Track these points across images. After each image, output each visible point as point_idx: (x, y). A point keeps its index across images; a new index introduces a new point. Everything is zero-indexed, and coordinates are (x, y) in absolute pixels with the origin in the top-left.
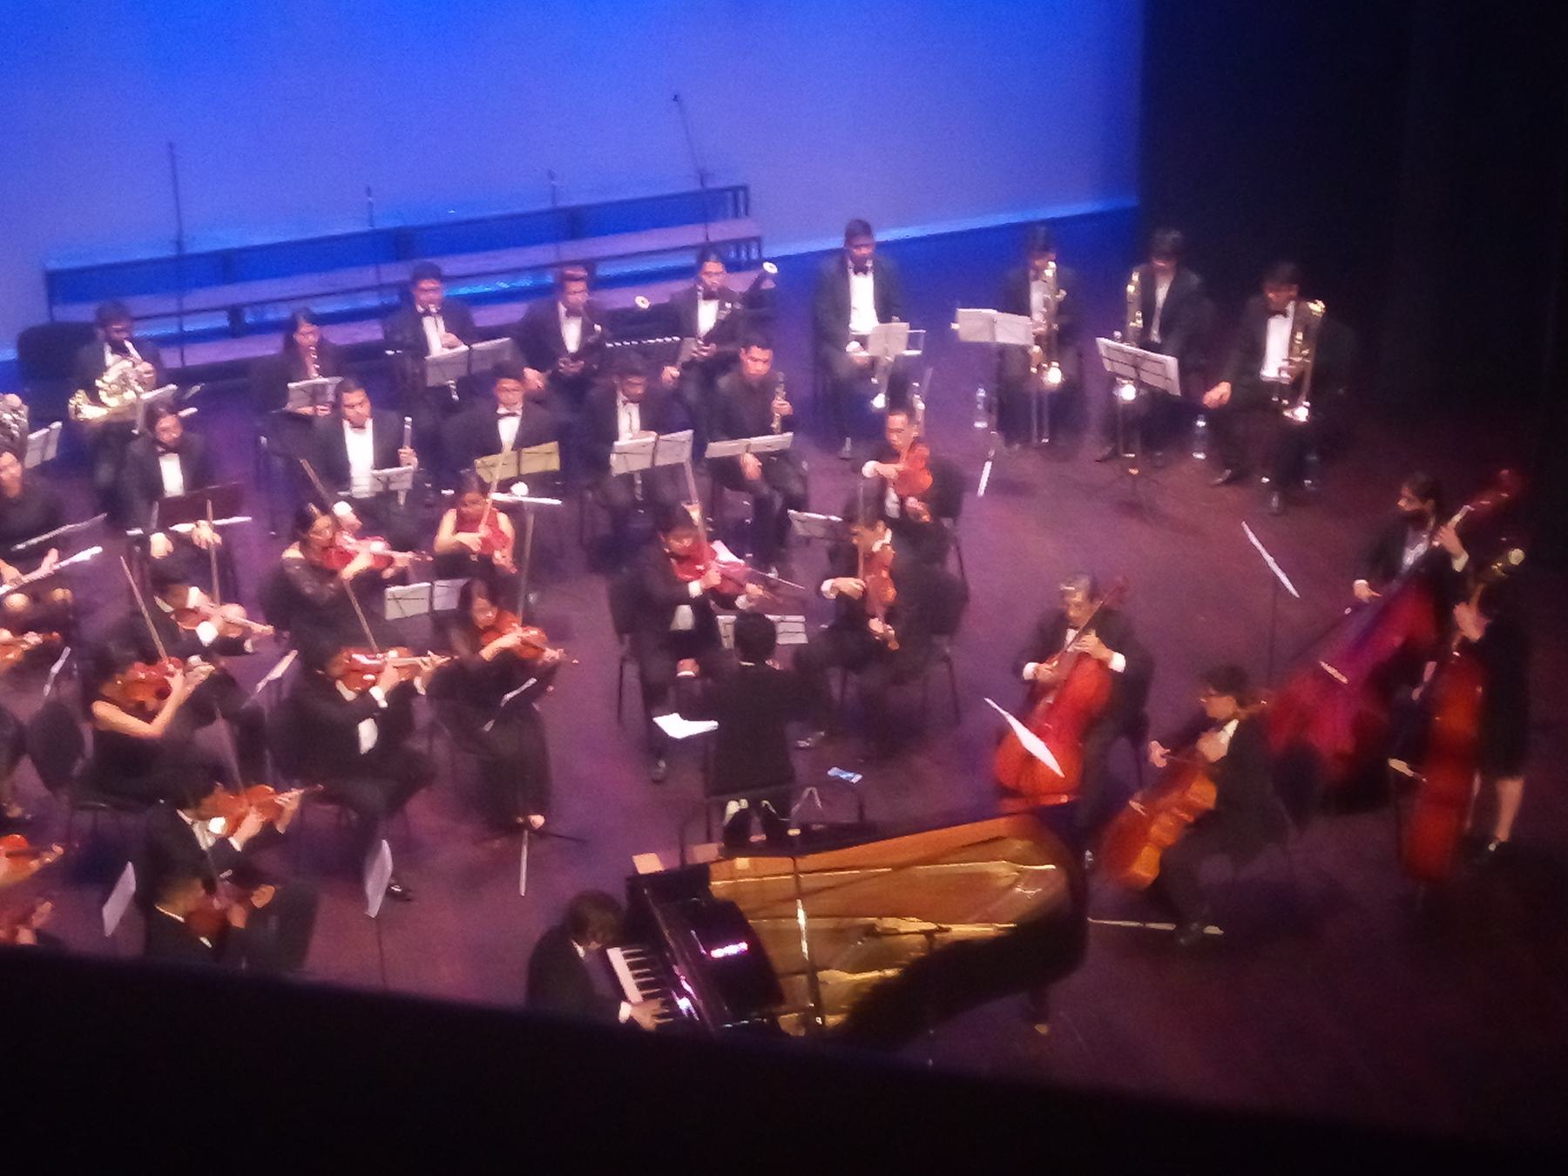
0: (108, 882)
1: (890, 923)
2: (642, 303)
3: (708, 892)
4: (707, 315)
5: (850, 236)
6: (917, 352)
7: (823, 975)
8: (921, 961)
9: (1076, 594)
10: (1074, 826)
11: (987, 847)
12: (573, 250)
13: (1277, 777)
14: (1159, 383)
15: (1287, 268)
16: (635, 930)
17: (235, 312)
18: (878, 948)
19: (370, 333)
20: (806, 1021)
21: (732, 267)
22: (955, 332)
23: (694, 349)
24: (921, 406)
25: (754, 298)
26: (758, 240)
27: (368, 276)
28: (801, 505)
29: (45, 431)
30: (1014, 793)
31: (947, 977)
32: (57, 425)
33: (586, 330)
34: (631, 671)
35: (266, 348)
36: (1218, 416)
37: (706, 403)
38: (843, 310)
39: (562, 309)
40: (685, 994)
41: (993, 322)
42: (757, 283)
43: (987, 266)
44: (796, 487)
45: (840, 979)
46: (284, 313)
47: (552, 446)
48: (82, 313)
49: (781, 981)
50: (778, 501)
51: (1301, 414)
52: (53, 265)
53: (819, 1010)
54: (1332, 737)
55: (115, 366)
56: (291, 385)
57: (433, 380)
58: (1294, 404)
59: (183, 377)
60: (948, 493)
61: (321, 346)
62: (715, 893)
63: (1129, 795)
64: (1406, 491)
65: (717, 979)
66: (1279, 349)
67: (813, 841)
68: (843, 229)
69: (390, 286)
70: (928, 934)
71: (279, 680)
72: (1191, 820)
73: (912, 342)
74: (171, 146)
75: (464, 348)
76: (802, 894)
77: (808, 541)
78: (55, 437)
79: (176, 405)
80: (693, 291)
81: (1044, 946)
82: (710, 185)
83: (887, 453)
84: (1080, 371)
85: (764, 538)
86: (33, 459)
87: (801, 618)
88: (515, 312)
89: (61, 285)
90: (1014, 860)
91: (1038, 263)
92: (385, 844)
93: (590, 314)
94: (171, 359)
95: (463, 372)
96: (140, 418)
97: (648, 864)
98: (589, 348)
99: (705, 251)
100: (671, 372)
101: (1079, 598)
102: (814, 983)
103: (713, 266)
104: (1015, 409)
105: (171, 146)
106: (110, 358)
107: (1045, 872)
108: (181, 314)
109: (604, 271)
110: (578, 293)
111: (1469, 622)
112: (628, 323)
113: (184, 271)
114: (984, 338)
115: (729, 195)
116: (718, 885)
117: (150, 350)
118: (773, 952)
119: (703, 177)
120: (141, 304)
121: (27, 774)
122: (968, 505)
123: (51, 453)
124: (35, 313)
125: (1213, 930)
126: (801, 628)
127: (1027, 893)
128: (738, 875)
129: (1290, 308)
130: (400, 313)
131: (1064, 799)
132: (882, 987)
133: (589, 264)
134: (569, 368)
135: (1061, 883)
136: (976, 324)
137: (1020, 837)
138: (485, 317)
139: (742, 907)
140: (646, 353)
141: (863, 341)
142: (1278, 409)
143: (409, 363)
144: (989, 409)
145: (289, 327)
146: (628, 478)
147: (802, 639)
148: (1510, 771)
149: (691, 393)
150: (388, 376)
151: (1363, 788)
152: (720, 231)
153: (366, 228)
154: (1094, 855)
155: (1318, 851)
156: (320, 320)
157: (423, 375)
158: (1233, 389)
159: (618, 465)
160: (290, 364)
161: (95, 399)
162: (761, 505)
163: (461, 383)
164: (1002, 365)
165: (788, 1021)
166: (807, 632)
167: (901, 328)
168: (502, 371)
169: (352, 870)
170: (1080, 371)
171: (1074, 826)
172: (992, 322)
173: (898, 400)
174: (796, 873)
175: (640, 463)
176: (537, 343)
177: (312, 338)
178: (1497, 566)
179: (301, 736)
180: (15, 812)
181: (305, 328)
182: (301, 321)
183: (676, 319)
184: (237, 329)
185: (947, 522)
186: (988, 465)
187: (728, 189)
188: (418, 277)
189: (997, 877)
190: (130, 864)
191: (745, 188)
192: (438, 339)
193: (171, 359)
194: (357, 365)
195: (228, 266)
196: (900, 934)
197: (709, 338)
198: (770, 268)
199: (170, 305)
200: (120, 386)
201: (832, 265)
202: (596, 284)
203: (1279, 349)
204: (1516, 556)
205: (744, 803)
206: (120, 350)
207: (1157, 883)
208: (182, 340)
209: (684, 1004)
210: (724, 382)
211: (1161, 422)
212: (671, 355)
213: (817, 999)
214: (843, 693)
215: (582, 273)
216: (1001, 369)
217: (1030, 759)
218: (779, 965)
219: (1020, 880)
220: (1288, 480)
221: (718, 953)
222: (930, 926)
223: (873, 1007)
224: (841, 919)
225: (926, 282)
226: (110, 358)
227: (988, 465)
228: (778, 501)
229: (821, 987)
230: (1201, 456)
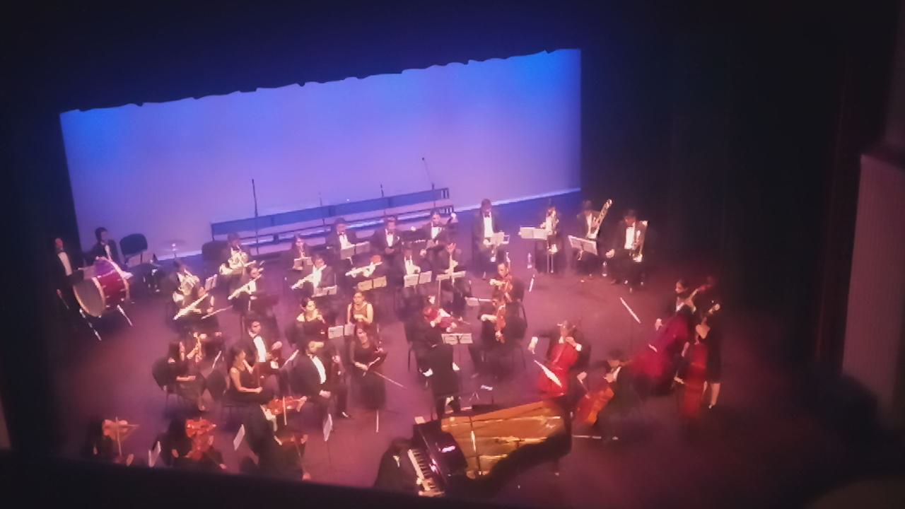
0: (235, 430)
1: (504, 438)
2: (413, 229)
3: (440, 429)
4: (435, 232)
5: (483, 204)
6: (507, 243)
7: (481, 457)
8: (514, 452)
9: (563, 326)
10: (567, 402)
11: (536, 411)
12: (389, 211)
13: (637, 384)
14: (590, 251)
15: (632, 211)
16: (416, 443)
17: (276, 236)
18: (498, 447)
19: (321, 241)
20: (476, 473)
21: (443, 215)
22: (520, 236)
23: (430, 244)
24: (508, 260)
25: (450, 226)
26: (452, 206)
27: (320, 222)
28: (469, 296)
29: (211, 278)
30: (544, 392)
31: (524, 457)
32: (216, 276)
33: (395, 238)
34: (413, 354)
35: (286, 247)
36: (609, 261)
37: (434, 262)
38: (481, 229)
39: (387, 231)
40: (432, 464)
41: (532, 231)
42: (450, 220)
43: (532, 212)
44: (467, 289)
45: (487, 459)
46: (290, 236)
47: (384, 278)
48: (224, 237)
49: (467, 460)
50: (462, 295)
51: (639, 259)
52: (214, 221)
53: (480, 469)
54: (655, 371)
55: (235, 255)
56: (296, 260)
57: (343, 257)
58: (636, 256)
59: (258, 258)
60: (518, 291)
61: (305, 246)
62: (443, 429)
63: (586, 393)
64: (678, 285)
65: (445, 460)
66: (632, 237)
67: (478, 409)
68: (481, 202)
69: (328, 225)
70: (517, 442)
71: (292, 362)
72: (606, 401)
73: (505, 239)
74: (253, 181)
75: (354, 245)
76: (472, 428)
77: (471, 308)
78: (215, 280)
79: (258, 267)
80: (430, 224)
81: (557, 445)
82: (436, 188)
83: (498, 277)
84: (563, 247)
85: (457, 306)
86: (208, 287)
87: (470, 334)
88: (370, 233)
89: (216, 228)
90: (546, 415)
91: (549, 211)
92: (330, 416)
93: (396, 233)
94: (254, 252)
95: (353, 254)
96: (244, 272)
97: (420, 420)
98: (396, 244)
99: (433, 211)
100: (423, 252)
101: (564, 327)
102: (478, 458)
103: (435, 216)
104: (541, 261)
105: (253, 181)
106: (233, 252)
107: (557, 419)
108: (257, 237)
109: (400, 218)
110: (392, 226)
111: (702, 331)
112: (408, 236)
113: (258, 222)
114: (530, 237)
115: (442, 192)
116: (444, 427)
117: (246, 249)
118: (465, 450)
119: (433, 186)
120: (243, 234)
121: (207, 395)
122: (525, 292)
123: (214, 285)
124: (209, 239)
125: (616, 438)
126: (471, 338)
127: (551, 427)
128: (451, 423)
129: (634, 224)
130: (332, 235)
131: (562, 394)
132: (502, 460)
133: (395, 216)
134: (389, 251)
135: (563, 421)
136: (526, 232)
137: (547, 407)
138: (360, 235)
139: (453, 434)
140: (415, 245)
141: (489, 239)
142: (632, 258)
143: (335, 252)
144: (532, 261)
145: (293, 240)
146: (411, 288)
147: (471, 342)
148: (716, 381)
149: (431, 258)
150: (327, 253)
151: (664, 388)
152: (439, 203)
153: (318, 205)
154: (574, 413)
155: (653, 410)
156: (303, 237)
157: (340, 255)
158: (616, 251)
159: (407, 285)
160: (294, 252)
161: (228, 266)
162: (456, 295)
163: (353, 257)
164: (538, 249)
165: (470, 474)
166: (473, 339)
167: (502, 234)
169: (320, 427)
170: (563, 247)
171: (567, 402)
172: (532, 231)
173: (501, 258)
174: (471, 422)
175: (414, 283)
176: (378, 242)
177: (302, 244)
178: (711, 311)
179: (299, 380)
180: (203, 408)
181: (299, 240)
182: (297, 237)
183: (424, 233)
184: (276, 241)
185: (519, 300)
187: (440, 190)
188: (338, 222)
189: (539, 421)
190: (243, 426)
191: (447, 189)
192: (344, 243)
193: (254, 252)
194: (313, 251)
195: (273, 220)
196: (507, 442)
197: (435, 240)
198: (454, 215)
199: (253, 234)
200: (237, 261)
201: (477, 215)
202: (398, 223)
203: (632, 237)
204: (717, 307)
205: (452, 398)
206: (236, 249)
207: (596, 424)
208: (257, 246)
209: (433, 468)
210: (441, 254)
211: (590, 264)
212: (423, 246)
213: (479, 466)
214: (485, 359)
215: (393, 219)
216: (536, 248)
217: (550, 381)
218: (466, 454)
219: (548, 423)
220: (635, 282)
221: (445, 450)
222: (518, 439)
223: (499, 467)
224: (483, 439)
225: (509, 218)
226: (233, 252)
227: (533, 280)
228: (462, 295)
229: (481, 462)
230: (605, 275)
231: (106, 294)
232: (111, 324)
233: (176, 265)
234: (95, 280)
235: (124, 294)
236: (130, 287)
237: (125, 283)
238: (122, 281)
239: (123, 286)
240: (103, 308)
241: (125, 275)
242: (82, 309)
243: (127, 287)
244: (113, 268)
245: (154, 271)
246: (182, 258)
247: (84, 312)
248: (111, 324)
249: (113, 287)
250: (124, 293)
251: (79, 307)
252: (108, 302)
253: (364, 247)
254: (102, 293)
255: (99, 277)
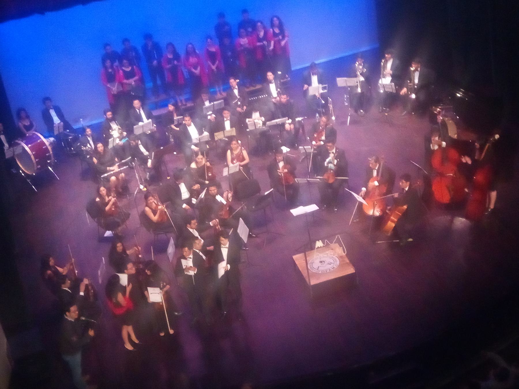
6: (326, 91)
136: (341, 82)
168: (224, 109)
186: (349, 117)
231: (36, 158)
232: (43, 179)
233: (83, 130)
234: (27, 148)
235: (49, 158)
236: (53, 149)
237: (50, 148)
238: (47, 148)
239: (49, 152)
240: (35, 168)
241: (47, 142)
242: (22, 170)
243: (51, 153)
244: (40, 138)
245: (70, 137)
246: (89, 127)
247: (24, 172)
248: (43, 179)
249: (40, 151)
250: (50, 156)
251: (19, 168)
252: (38, 163)
253: (220, 103)
254: (32, 157)
255: (30, 145)
